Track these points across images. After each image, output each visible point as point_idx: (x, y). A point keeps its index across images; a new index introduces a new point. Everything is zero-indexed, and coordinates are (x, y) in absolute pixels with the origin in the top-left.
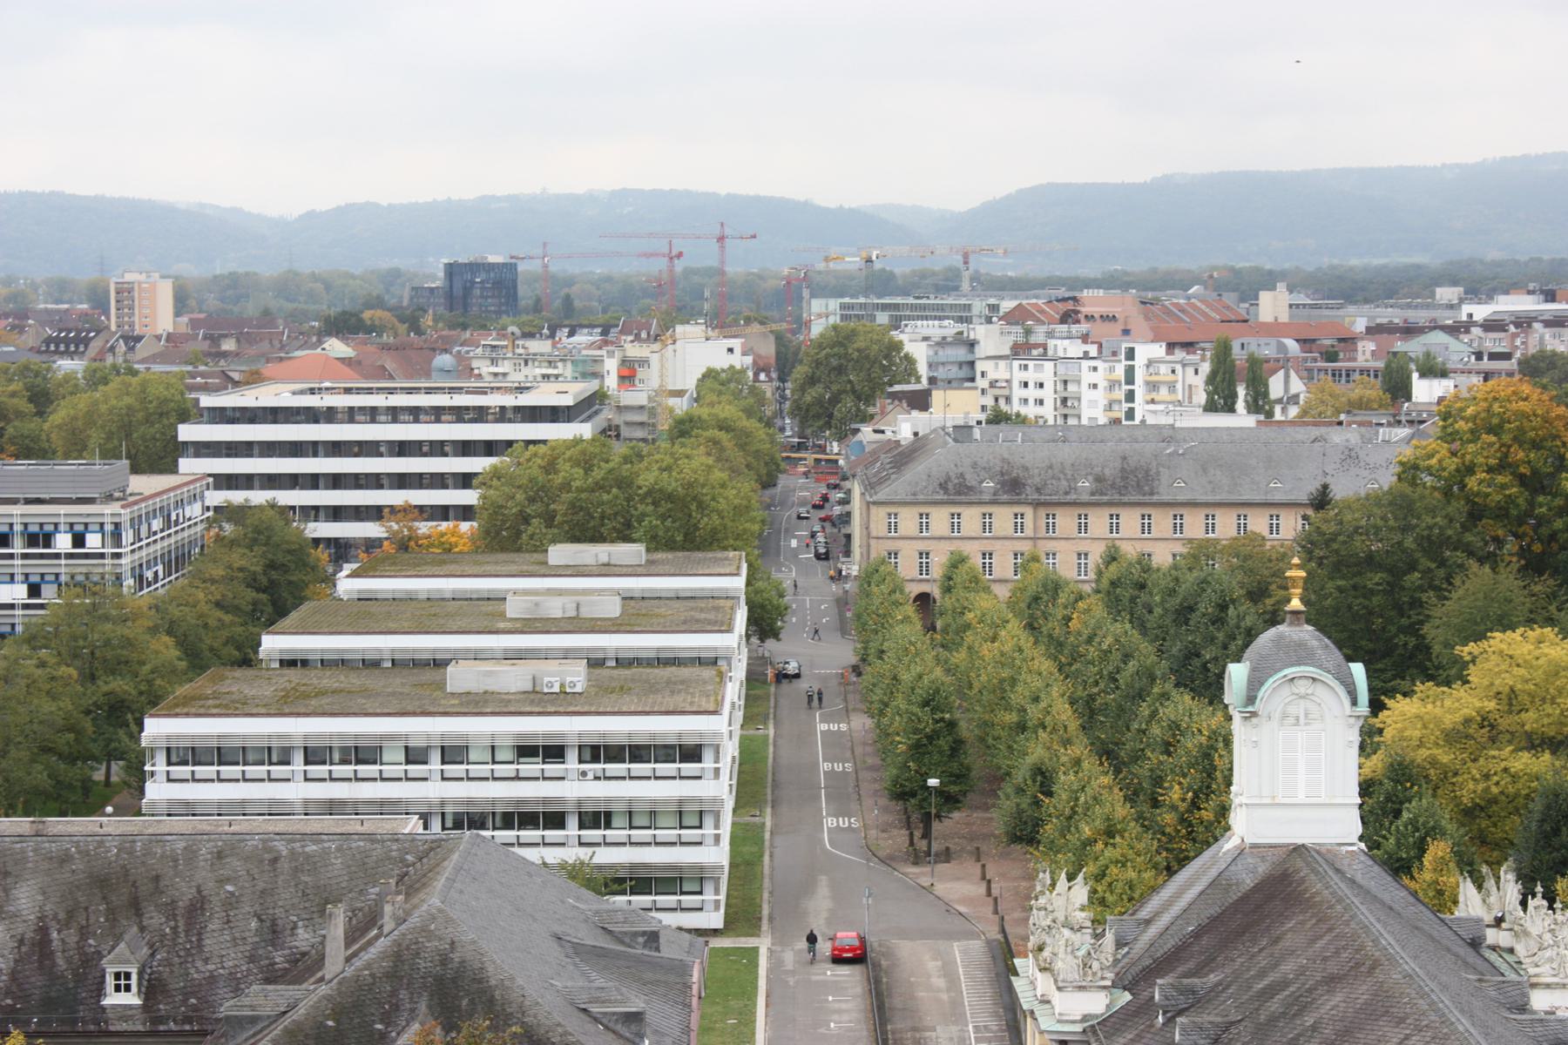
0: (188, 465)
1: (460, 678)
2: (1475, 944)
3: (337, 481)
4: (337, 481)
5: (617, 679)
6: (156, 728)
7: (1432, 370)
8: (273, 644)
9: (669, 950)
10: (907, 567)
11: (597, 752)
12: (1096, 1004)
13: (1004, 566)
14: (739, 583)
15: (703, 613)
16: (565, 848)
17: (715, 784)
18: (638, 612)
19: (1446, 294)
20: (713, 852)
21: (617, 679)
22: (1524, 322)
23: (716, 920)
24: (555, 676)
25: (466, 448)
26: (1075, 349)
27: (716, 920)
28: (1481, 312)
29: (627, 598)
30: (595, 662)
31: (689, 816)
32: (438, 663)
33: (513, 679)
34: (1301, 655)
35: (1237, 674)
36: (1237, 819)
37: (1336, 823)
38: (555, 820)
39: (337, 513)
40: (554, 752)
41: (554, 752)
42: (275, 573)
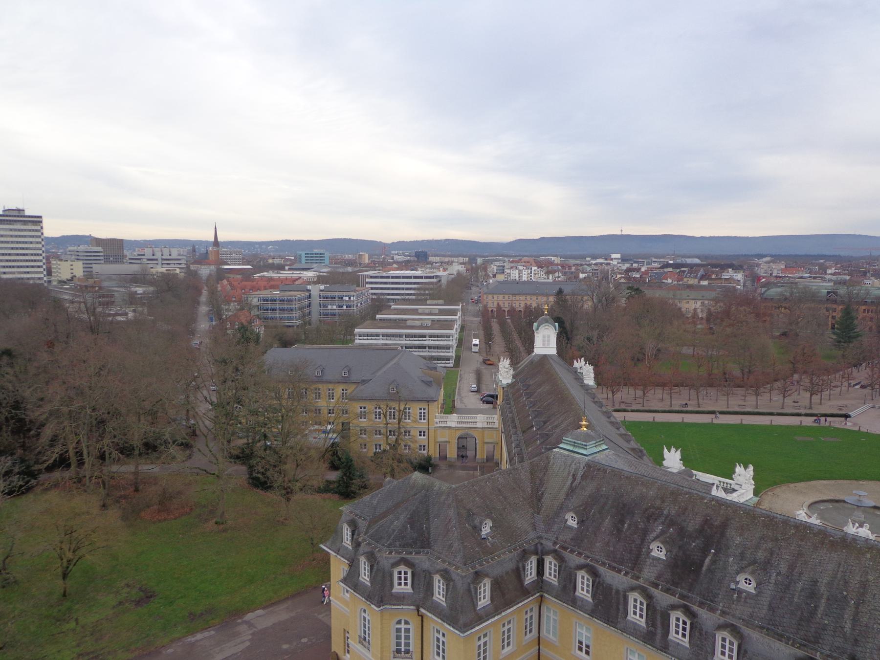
0: (367, 286)
1: (409, 323)
2: (576, 372)
3: (393, 289)
4: (393, 289)
5: (436, 324)
6: (357, 330)
7: (583, 272)
8: (378, 316)
9: (438, 370)
10: (490, 305)
11: (431, 336)
12: (510, 381)
13: (506, 305)
14: (460, 307)
15: (454, 312)
16: (426, 353)
17: (453, 343)
18: (441, 312)
19: (588, 259)
20: (452, 353)
21: (436, 324)
22: (601, 264)
23: (452, 365)
24: (425, 323)
25: (415, 283)
26: (521, 268)
27: (452, 365)
28: (594, 262)
29: (440, 310)
30: (433, 320)
31: (447, 347)
32: (406, 320)
33: (418, 323)
34: (547, 322)
35: (535, 324)
36: (535, 350)
37: (552, 350)
38: (425, 348)
39: (393, 294)
40: (424, 336)
41: (424, 336)
42: (379, 304)
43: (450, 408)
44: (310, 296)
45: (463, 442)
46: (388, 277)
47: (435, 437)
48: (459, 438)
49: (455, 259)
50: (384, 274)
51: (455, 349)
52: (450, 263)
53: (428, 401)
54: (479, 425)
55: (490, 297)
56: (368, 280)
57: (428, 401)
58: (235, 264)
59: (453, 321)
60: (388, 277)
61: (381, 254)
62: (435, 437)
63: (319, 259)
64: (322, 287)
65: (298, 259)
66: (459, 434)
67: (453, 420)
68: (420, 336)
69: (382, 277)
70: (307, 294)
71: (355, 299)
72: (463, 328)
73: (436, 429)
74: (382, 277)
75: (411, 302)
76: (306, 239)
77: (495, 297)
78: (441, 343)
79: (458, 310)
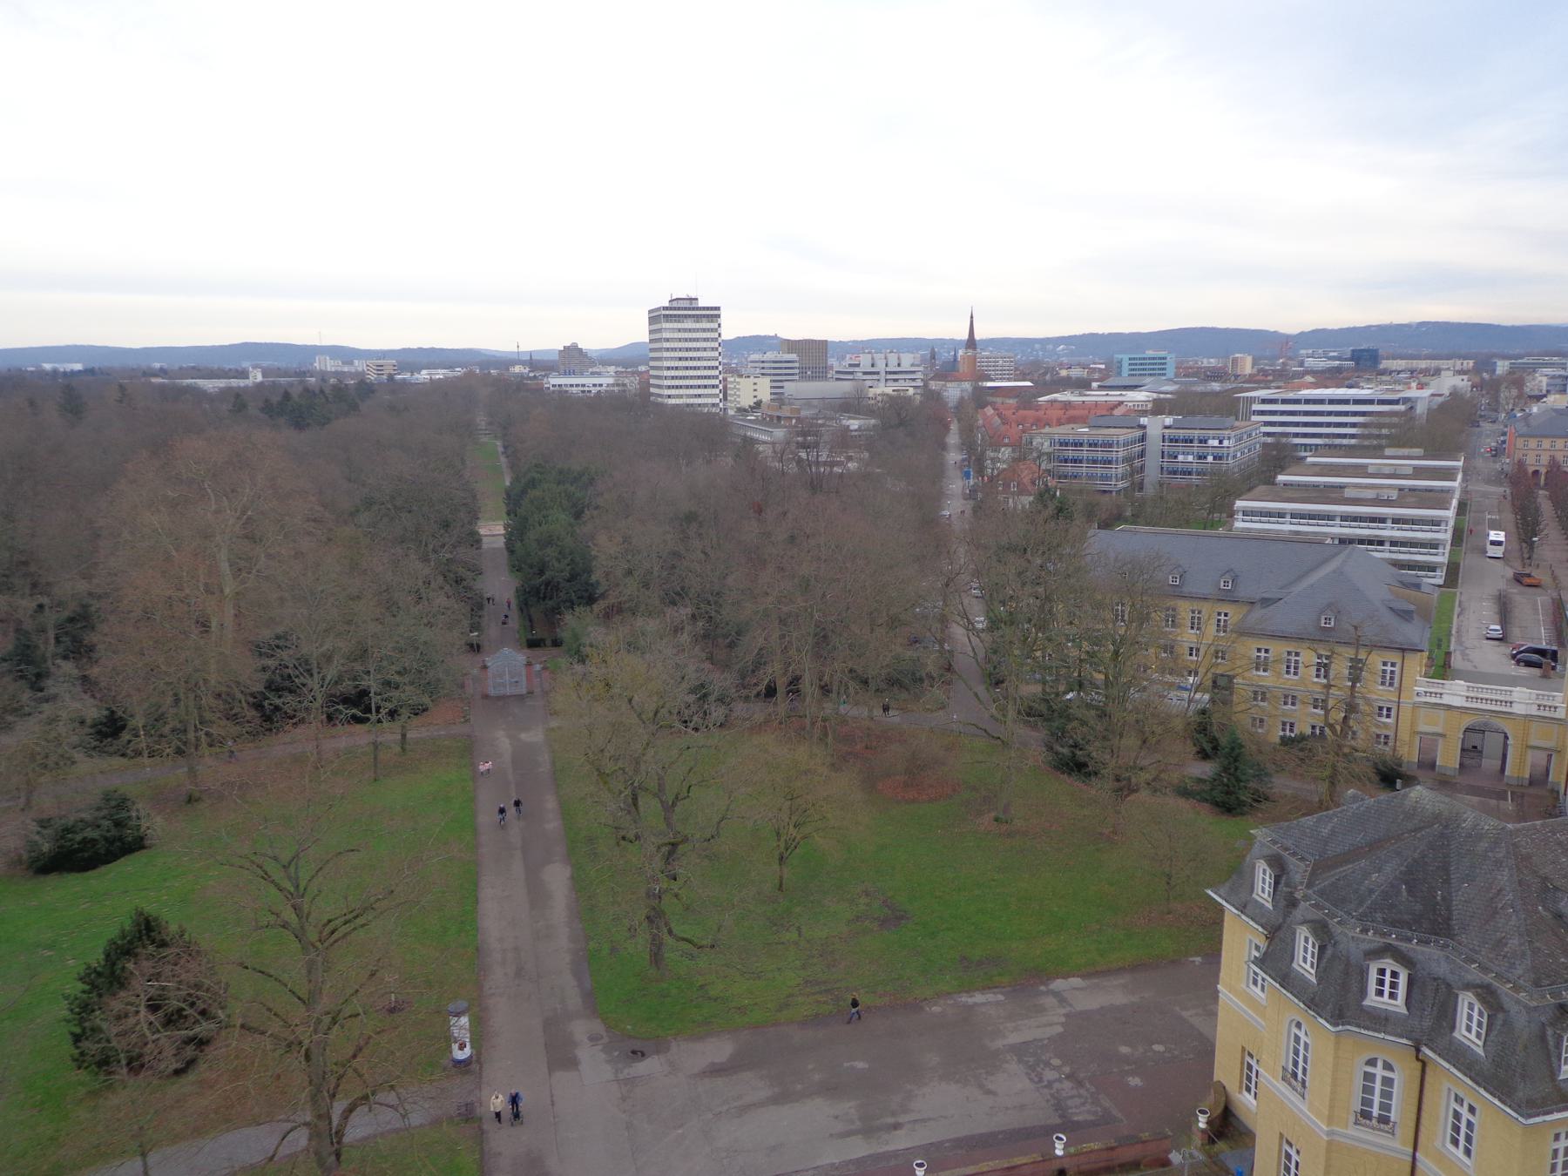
0: (1254, 418)
1: (1348, 493)
3: (1306, 424)
4: (1306, 424)
5: (1408, 496)
6: (1239, 504)
8: (1281, 478)
9: (1424, 589)
11: (1396, 521)
14: (1460, 464)
15: (1448, 474)
16: (1385, 553)
17: (1446, 536)
18: (1419, 473)
20: (1441, 557)
21: (1408, 496)
23: (1441, 581)
24: (1385, 494)
25: (1355, 414)
27: (1441, 581)
29: (1415, 468)
30: (1401, 489)
31: (1434, 545)
32: (1342, 487)
33: (1370, 494)
38: (1381, 543)
39: (1305, 435)
40: (1383, 520)
41: (1383, 520)
43: (1442, 668)
44: (1143, 439)
45: (1475, 739)
46: (1297, 402)
47: (1413, 724)
48: (1467, 730)
49: (1443, 364)
50: (1291, 395)
51: (1448, 547)
52: (1437, 372)
53: (1403, 650)
54: (1518, 709)
55: (1533, 443)
56: (1256, 407)
57: (1403, 650)
58: (1002, 379)
59: (1449, 491)
60: (1297, 402)
61: (1278, 357)
62: (1413, 724)
63: (1155, 368)
64: (1169, 421)
65: (1113, 368)
66: (1467, 721)
67: (1455, 693)
68: (1373, 519)
69: (1285, 401)
70: (1139, 433)
71: (1234, 444)
72: (1462, 508)
73: (1416, 706)
74: (1285, 401)
75: (1350, 451)
76: (1127, 331)
77: (1546, 443)
78: (1419, 535)
79: (1455, 468)
